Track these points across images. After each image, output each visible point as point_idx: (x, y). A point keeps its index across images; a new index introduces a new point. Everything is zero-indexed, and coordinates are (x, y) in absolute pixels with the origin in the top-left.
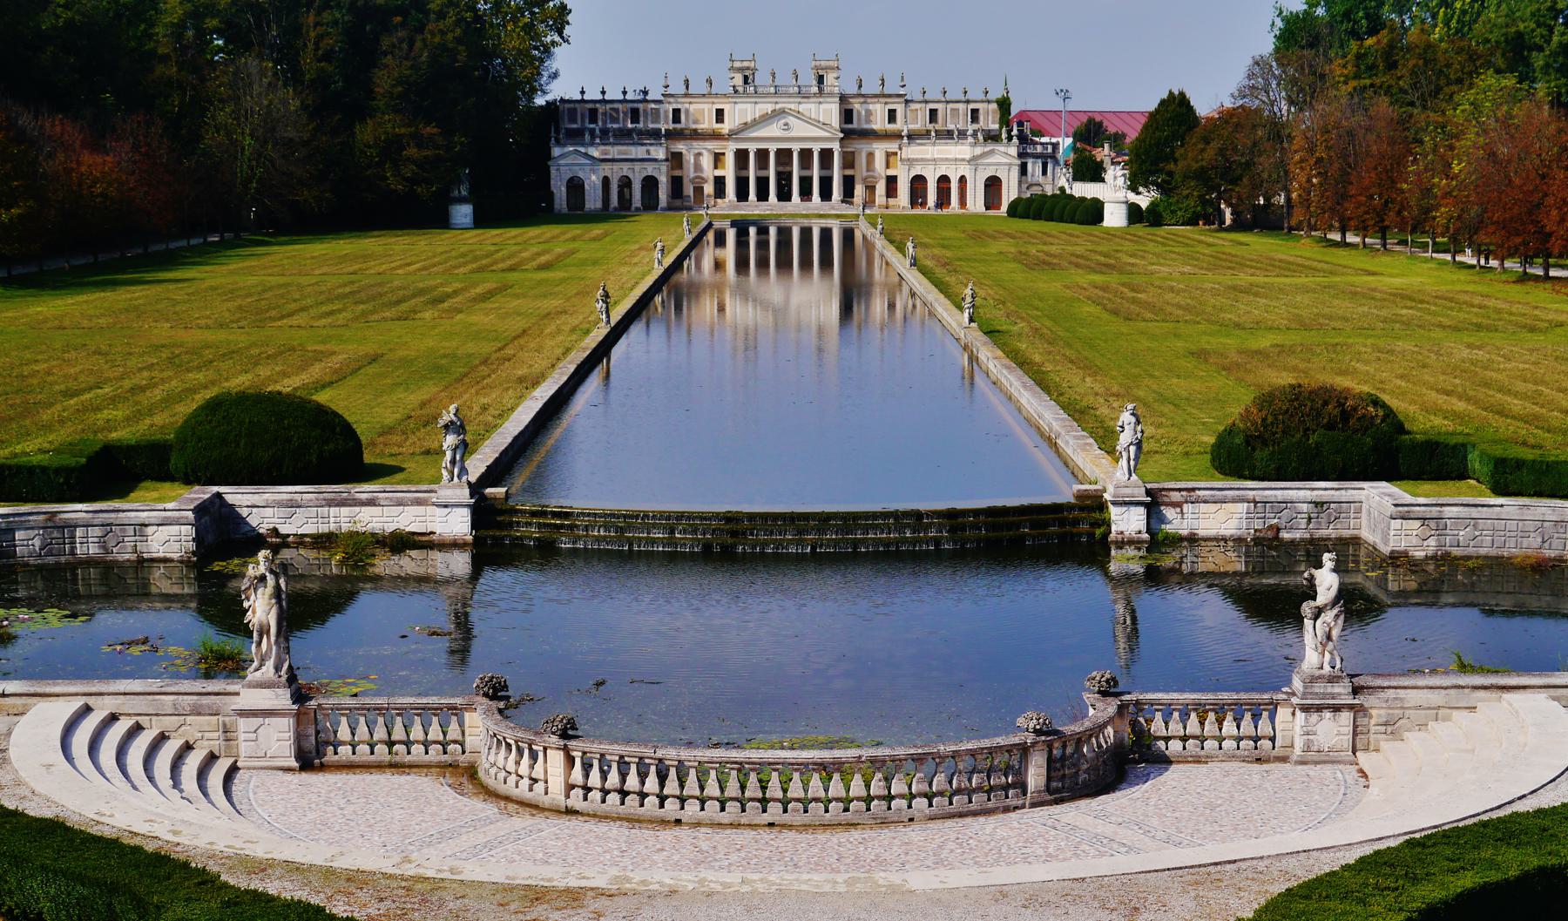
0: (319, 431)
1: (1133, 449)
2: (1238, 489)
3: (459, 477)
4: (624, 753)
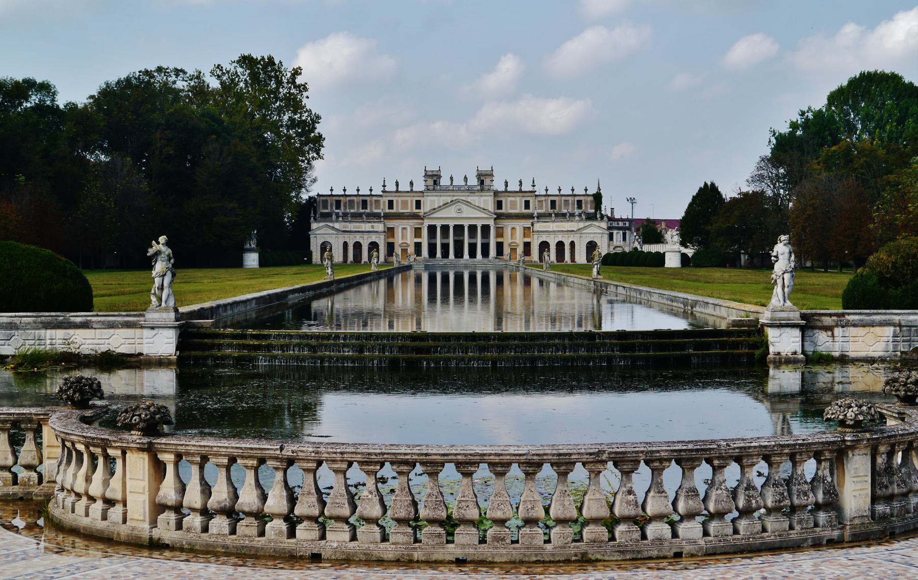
2: (885, 314)
3: (166, 302)
4: (236, 452)
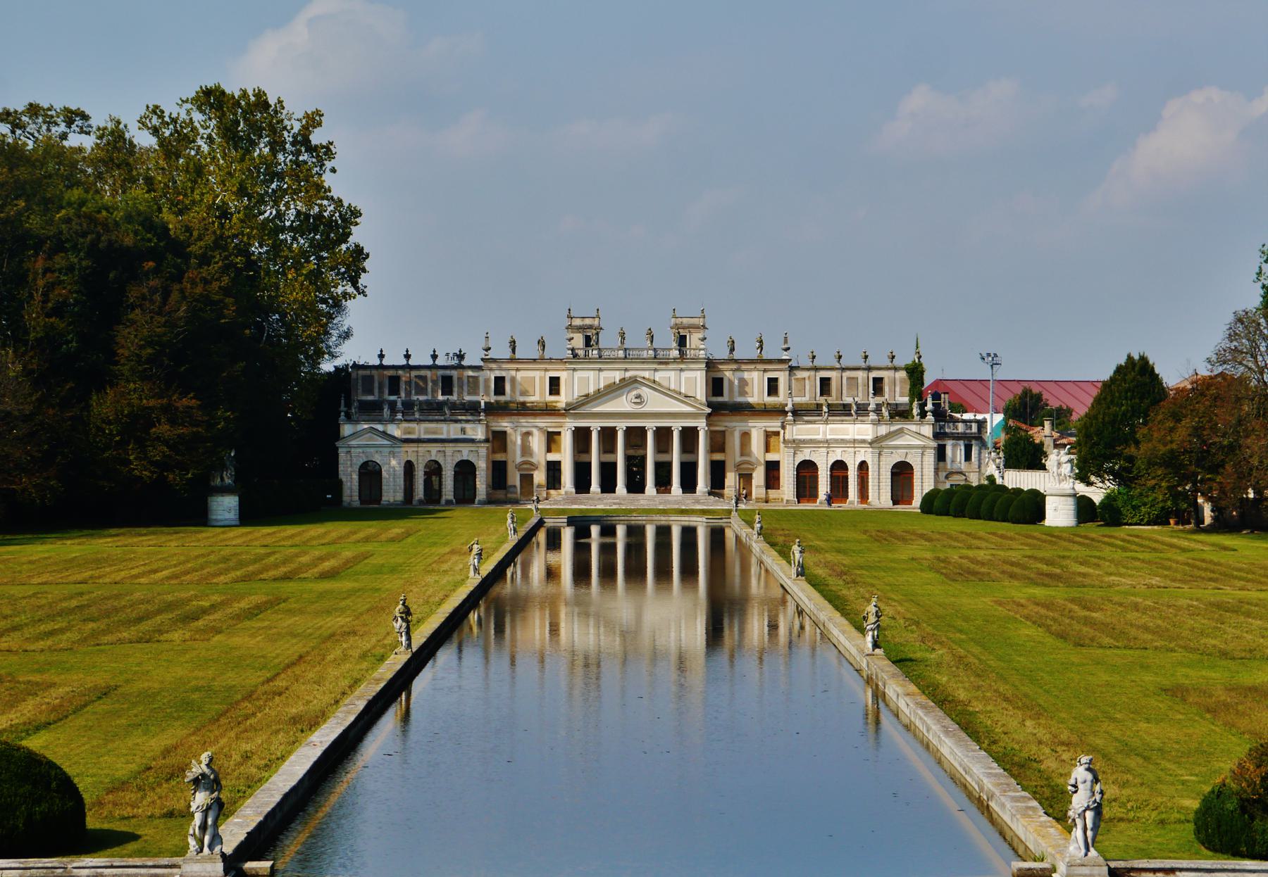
0: (28, 787)
1: (1089, 815)
3: (211, 847)
